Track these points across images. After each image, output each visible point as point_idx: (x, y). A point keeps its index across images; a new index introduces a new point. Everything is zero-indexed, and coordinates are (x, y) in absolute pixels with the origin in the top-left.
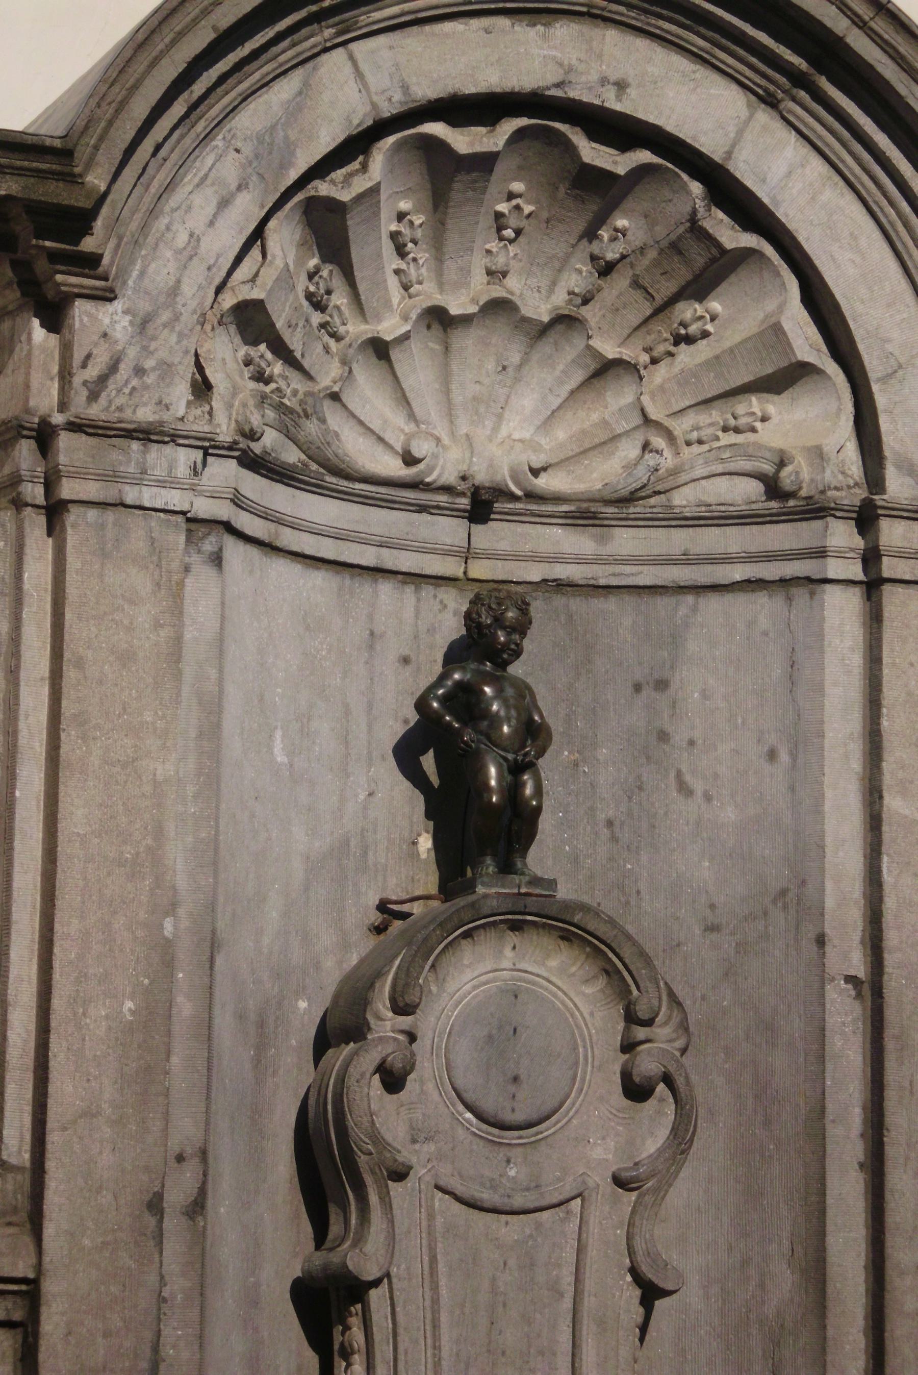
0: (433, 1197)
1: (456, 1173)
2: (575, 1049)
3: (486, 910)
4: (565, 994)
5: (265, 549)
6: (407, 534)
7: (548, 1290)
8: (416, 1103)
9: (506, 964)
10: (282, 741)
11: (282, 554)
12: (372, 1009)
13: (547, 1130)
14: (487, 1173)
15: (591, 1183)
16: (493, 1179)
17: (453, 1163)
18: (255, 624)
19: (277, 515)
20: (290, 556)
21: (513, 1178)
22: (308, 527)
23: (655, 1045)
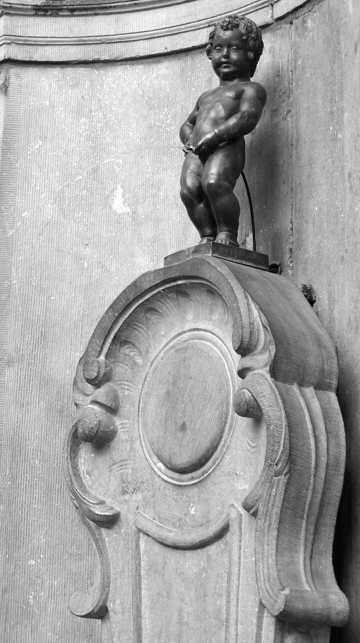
0: (138, 541)
1: (156, 517)
2: (221, 390)
3: (147, 286)
4: (222, 341)
5: (96, 65)
6: (226, 8)
7: (215, 619)
8: (127, 460)
9: (188, 327)
10: (123, 197)
11: (118, 63)
12: (78, 388)
13: (209, 469)
14: (177, 514)
15: (233, 515)
16: (181, 519)
17: (154, 508)
18: (83, 120)
19: (98, 38)
20: (129, 62)
21: (193, 515)
22: (138, 36)
23: (256, 372)
